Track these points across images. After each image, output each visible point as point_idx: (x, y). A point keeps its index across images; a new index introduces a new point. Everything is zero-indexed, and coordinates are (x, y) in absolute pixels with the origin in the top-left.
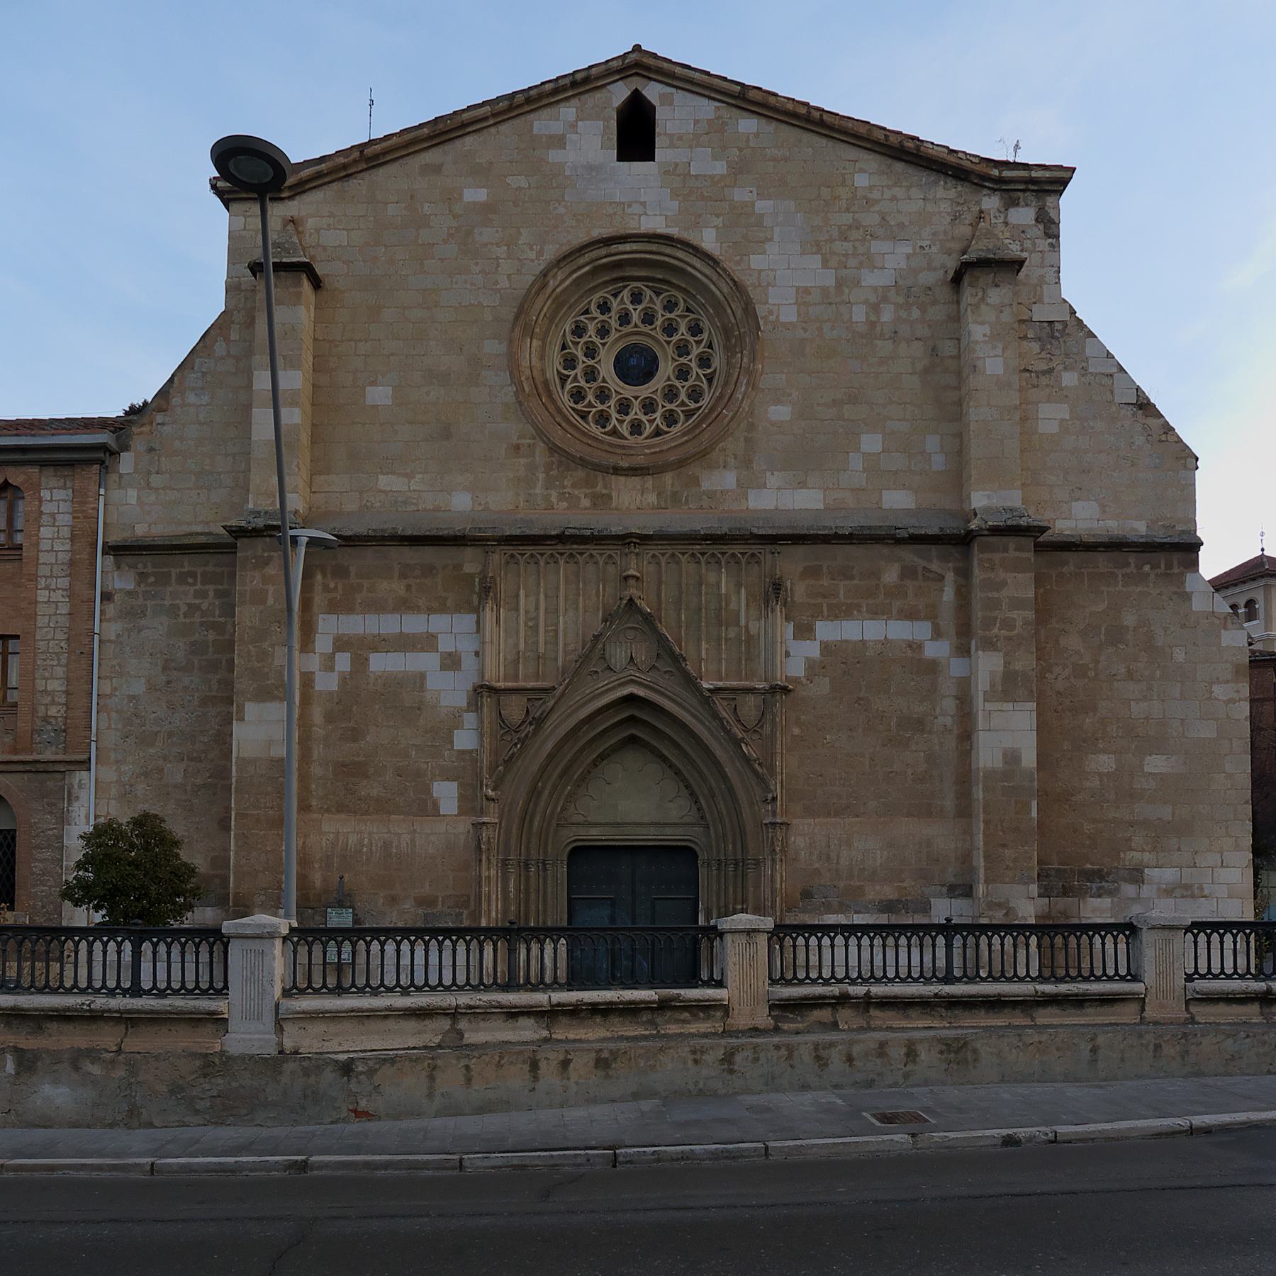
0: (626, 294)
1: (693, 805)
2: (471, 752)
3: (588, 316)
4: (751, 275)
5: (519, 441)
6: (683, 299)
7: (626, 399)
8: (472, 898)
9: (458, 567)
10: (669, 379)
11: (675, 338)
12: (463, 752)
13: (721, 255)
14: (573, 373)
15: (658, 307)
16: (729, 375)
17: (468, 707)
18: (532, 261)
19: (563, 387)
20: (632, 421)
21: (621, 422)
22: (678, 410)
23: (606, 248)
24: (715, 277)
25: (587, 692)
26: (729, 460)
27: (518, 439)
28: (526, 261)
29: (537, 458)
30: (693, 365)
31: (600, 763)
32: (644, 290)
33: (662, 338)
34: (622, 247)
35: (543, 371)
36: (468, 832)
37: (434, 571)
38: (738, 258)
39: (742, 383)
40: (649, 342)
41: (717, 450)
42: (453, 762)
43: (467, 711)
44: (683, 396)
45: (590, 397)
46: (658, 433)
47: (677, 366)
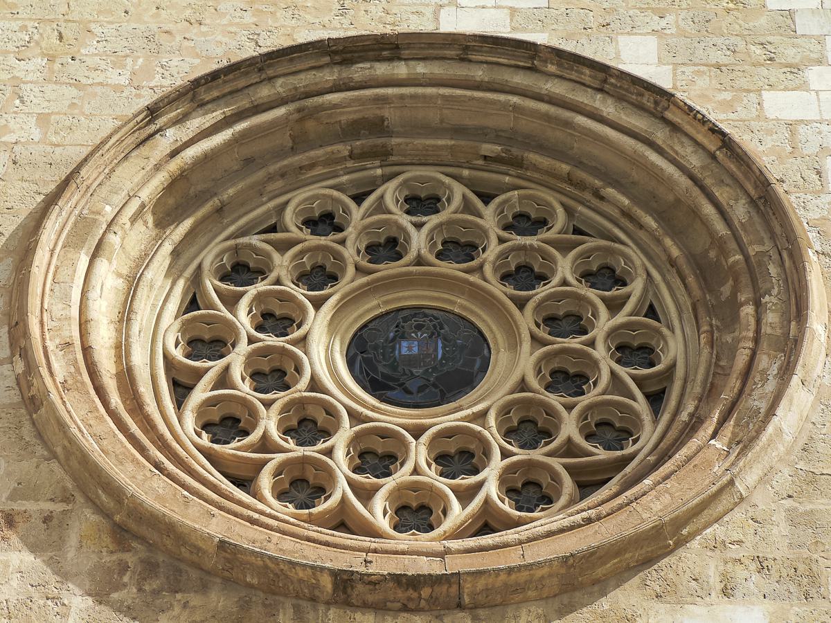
0: (390, 192)
3: (272, 236)
4: (769, 132)
5: (18, 506)
6: (563, 204)
7: (384, 434)
10: (522, 386)
11: (542, 291)
13: (675, 87)
14: (217, 366)
15: (489, 218)
16: (717, 373)
18: (118, 88)
19: (179, 404)
20: (400, 489)
21: (366, 494)
22: (556, 463)
23: (336, 69)
24: (660, 135)
26: (740, 573)
27: (12, 497)
28: (98, 89)
29: (71, 554)
30: (600, 353)
32: (449, 188)
33: (499, 290)
34: (381, 69)
35: (122, 350)
38: (727, 96)
39: (764, 373)
40: (459, 304)
41: (695, 544)
44: (570, 428)
45: (270, 423)
46: (487, 523)
47: (547, 357)
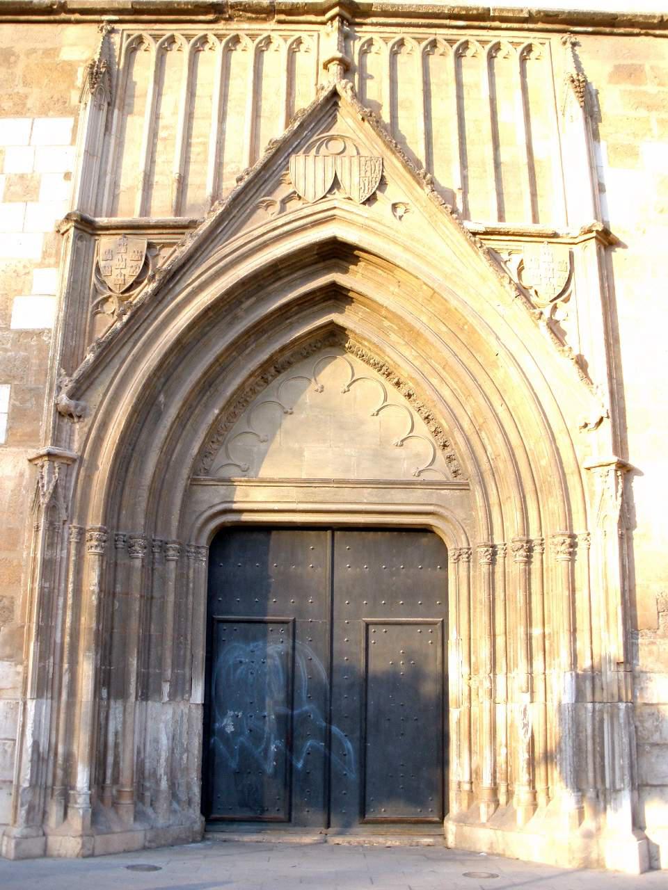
1: (439, 452)
2: (40, 333)
8: (19, 602)
9: (51, 52)
12: (27, 334)
17: (44, 258)
25: (256, 233)
31: (274, 377)
36: (22, 475)
37: (12, 59)
42: (6, 350)
43: (41, 265)
